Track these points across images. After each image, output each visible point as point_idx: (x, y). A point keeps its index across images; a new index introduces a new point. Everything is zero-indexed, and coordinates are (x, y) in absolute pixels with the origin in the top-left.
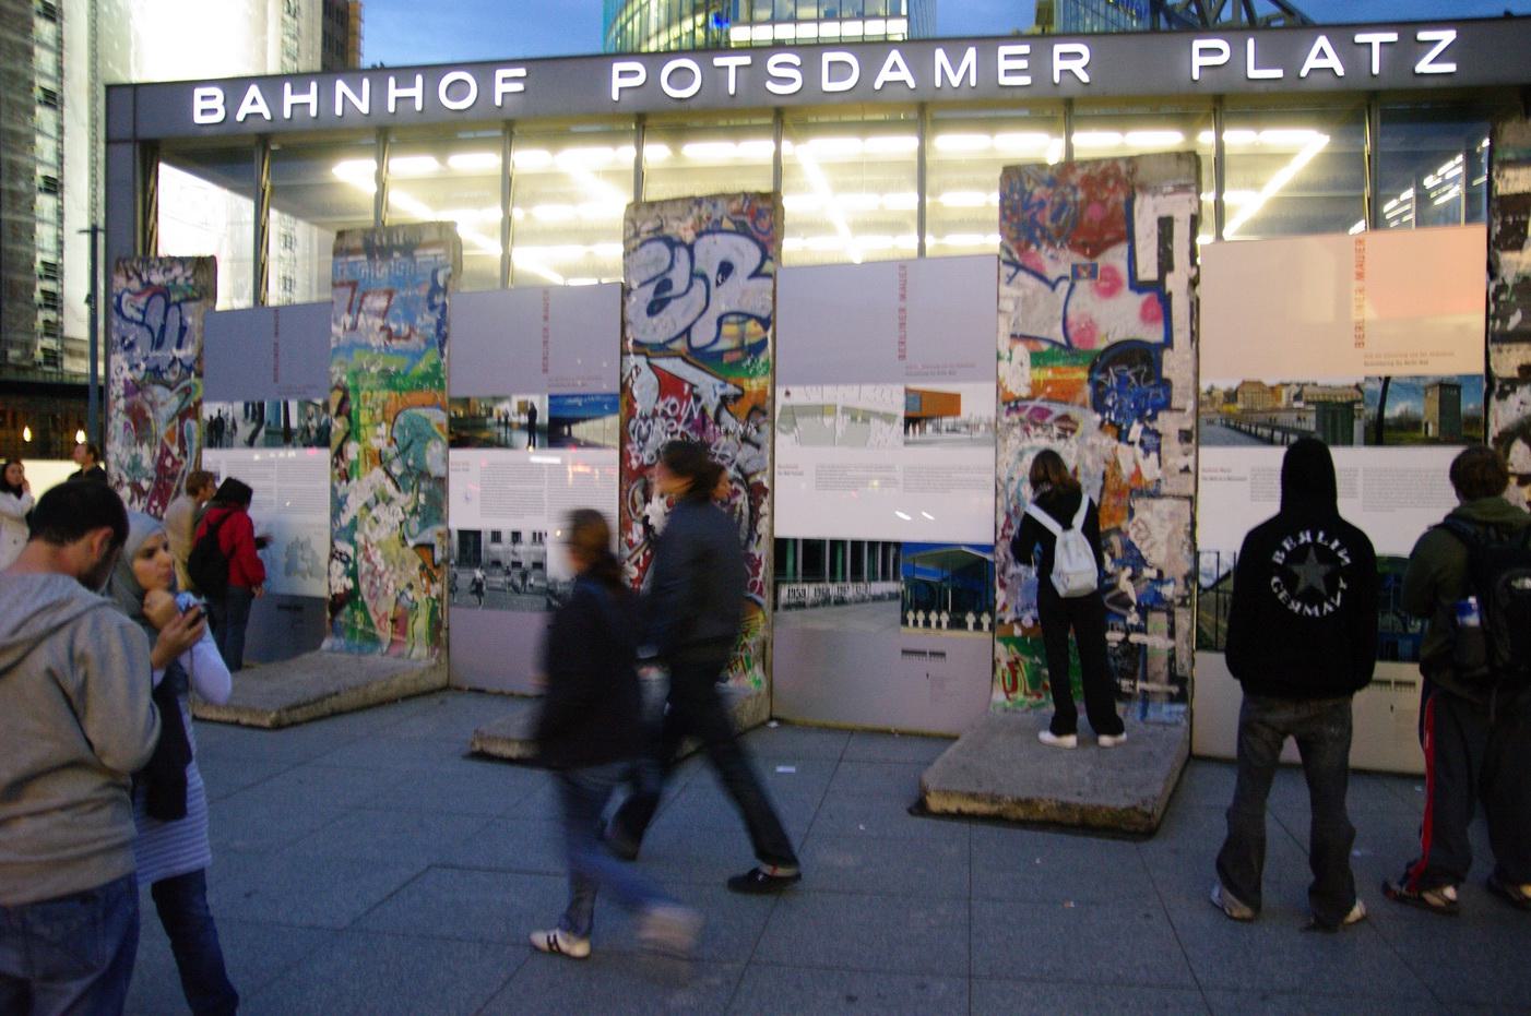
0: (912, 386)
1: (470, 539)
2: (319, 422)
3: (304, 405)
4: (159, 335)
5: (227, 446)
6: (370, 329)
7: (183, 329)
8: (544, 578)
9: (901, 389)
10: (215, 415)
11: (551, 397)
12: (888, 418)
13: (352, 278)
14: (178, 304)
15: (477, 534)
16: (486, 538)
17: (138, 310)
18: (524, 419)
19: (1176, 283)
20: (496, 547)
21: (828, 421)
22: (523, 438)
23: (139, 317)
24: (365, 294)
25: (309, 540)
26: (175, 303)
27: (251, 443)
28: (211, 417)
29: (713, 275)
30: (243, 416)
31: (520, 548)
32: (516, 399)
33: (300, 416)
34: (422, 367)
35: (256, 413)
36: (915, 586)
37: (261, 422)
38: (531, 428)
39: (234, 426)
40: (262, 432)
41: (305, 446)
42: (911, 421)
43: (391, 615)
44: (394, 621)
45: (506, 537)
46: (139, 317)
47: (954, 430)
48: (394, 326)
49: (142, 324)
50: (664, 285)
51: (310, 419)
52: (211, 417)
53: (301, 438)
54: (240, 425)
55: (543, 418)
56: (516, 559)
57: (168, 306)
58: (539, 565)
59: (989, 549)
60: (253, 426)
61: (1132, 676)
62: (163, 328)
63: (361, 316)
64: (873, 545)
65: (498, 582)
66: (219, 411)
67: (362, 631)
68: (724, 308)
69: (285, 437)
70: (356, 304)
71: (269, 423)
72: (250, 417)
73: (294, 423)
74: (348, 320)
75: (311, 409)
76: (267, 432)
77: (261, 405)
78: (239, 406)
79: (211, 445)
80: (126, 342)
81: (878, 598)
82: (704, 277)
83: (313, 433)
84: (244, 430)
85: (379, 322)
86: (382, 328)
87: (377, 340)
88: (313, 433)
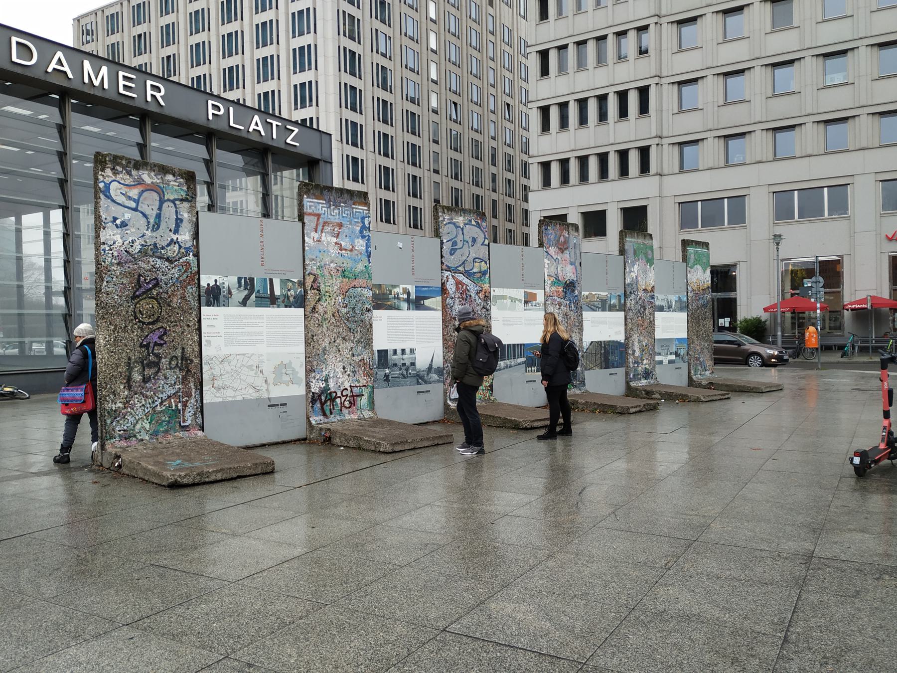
2: (295, 292)
3: (284, 282)
6: (329, 243)
7: (179, 221)
10: (212, 283)
14: (173, 201)
23: (133, 205)
26: (168, 200)
27: (244, 303)
28: (208, 285)
30: (237, 286)
33: (282, 288)
35: (248, 284)
39: (230, 292)
40: (253, 296)
41: (286, 307)
46: (133, 205)
48: (343, 244)
49: (136, 210)
51: (289, 290)
52: (208, 285)
53: (283, 302)
60: (246, 292)
62: (158, 216)
63: (324, 234)
66: (216, 281)
69: (273, 300)
70: (320, 228)
71: (258, 292)
72: (243, 288)
73: (277, 292)
74: (316, 236)
75: (290, 284)
77: (252, 280)
78: (233, 280)
83: (291, 299)
85: (334, 240)
86: (336, 243)
87: (334, 251)
88: (291, 299)
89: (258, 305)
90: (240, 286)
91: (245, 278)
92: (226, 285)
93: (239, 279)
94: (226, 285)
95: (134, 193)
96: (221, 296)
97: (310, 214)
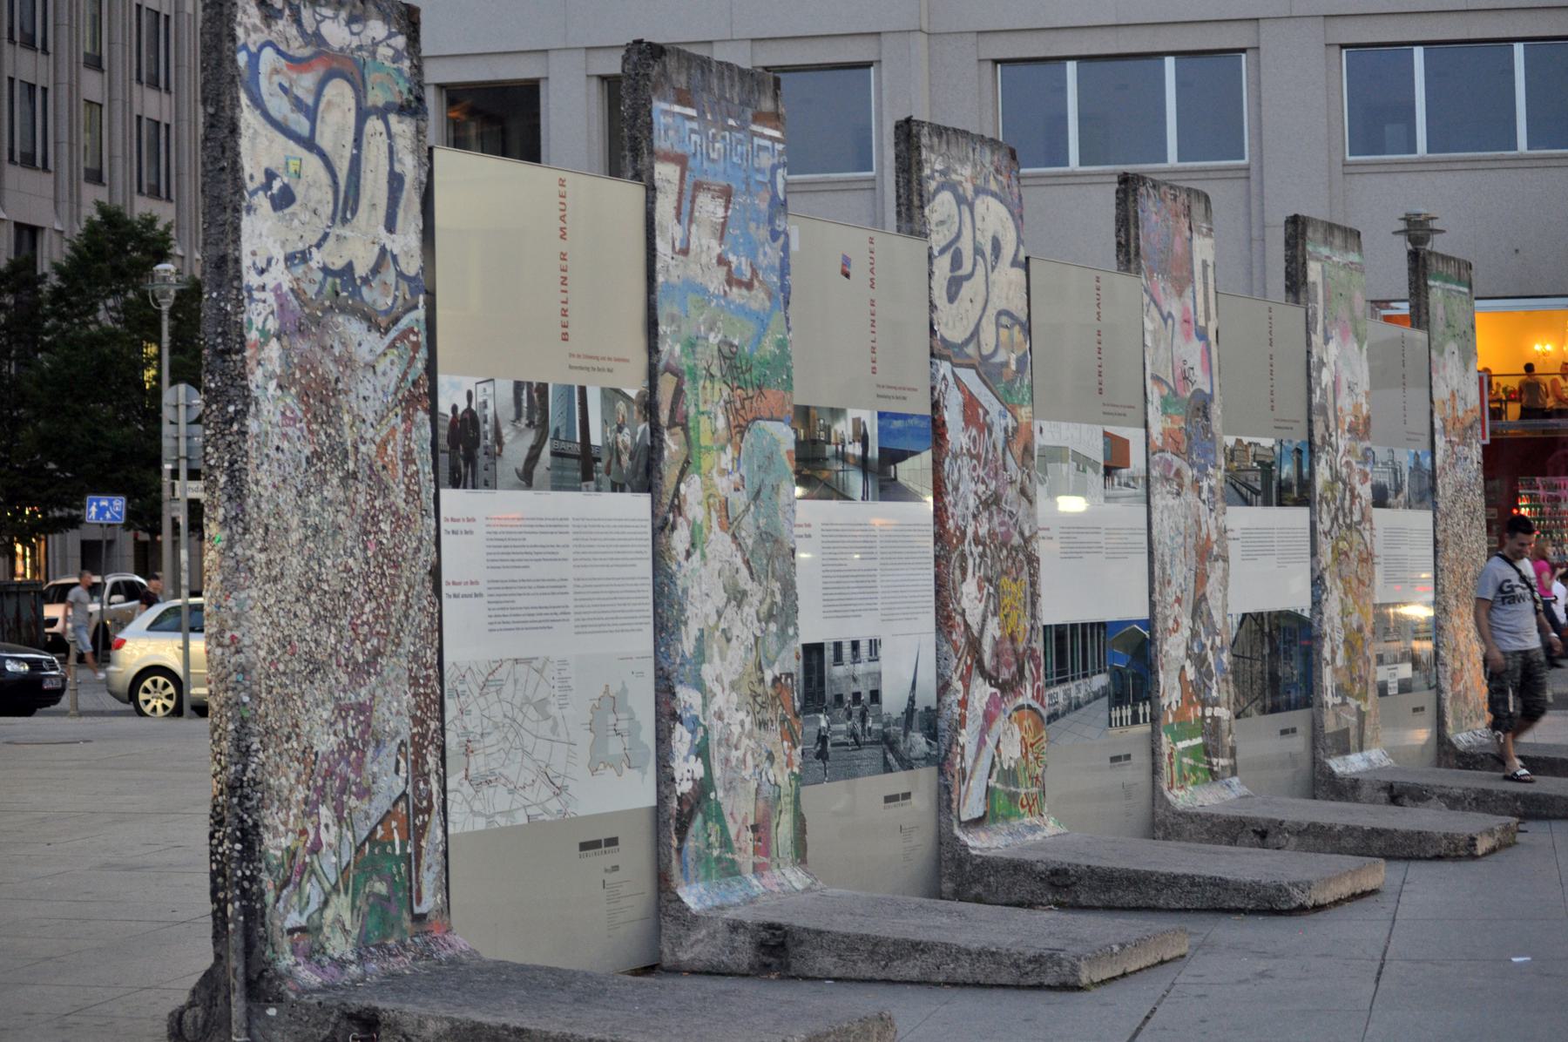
0: (1111, 429)
1: (813, 652)
4: (348, 186)
5: (486, 485)
8: (878, 717)
9: (1099, 430)
10: (462, 407)
11: (881, 415)
12: (1094, 465)
13: (678, 150)
15: (819, 648)
16: (829, 654)
17: (298, 104)
18: (855, 449)
19: (1212, 336)
20: (839, 671)
21: (1064, 467)
22: (855, 480)
23: (301, 125)
24: (698, 186)
25: (624, 691)
27: (526, 478)
28: (455, 408)
29: (988, 249)
30: (512, 415)
31: (861, 668)
32: (852, 413)
33: (605, 422)
34: (769, 346)
36: (1117, 675)
37: (542, 427)
38: (864, 464)
39: (498, 439)
42: (1109, 471)
43: (751, 821)
44: (755, 828)
45: (847, 651)
46: (301, 125)
47: (1127, 485)
49: (309, 144)
50: (956, 262)
51: (620, 429)
52: (455, 408)
54: (507, 433)
55: (874, 453)
56: (856, 689)
57: (362, 115)
58: (875, 696)
59: (1149, 624)
60: (530, 438)
61: (1216, 756)
62: (356, 162)
63: (694, 228)
64: (1092, 624)
65: (840, 732)
66: (469, 395)
67: (719, 860)
68: (1003, 305)
72: (524, 421)
73: (596, 439)
76: (554, 454)
77: (542, 389)
79: (455, 483)
80: (277, 185)
81: (1097, 696)
82: (983, 256)
84: (517, 445)
87: (715, 281)
89: (559, 485)
90: (518, 416)
91: (530, 384)
92: (490, 412)
93: (518, 386)
94: (490, 412)
95: (305, 84)
96: (480, 451)
97: (668, 158)
